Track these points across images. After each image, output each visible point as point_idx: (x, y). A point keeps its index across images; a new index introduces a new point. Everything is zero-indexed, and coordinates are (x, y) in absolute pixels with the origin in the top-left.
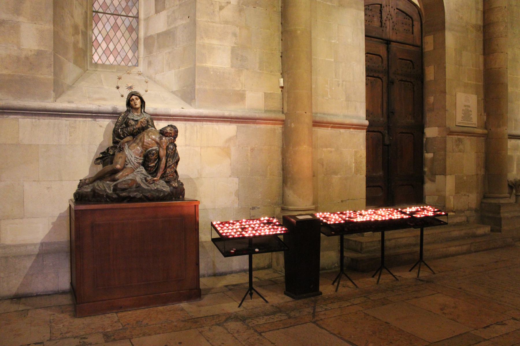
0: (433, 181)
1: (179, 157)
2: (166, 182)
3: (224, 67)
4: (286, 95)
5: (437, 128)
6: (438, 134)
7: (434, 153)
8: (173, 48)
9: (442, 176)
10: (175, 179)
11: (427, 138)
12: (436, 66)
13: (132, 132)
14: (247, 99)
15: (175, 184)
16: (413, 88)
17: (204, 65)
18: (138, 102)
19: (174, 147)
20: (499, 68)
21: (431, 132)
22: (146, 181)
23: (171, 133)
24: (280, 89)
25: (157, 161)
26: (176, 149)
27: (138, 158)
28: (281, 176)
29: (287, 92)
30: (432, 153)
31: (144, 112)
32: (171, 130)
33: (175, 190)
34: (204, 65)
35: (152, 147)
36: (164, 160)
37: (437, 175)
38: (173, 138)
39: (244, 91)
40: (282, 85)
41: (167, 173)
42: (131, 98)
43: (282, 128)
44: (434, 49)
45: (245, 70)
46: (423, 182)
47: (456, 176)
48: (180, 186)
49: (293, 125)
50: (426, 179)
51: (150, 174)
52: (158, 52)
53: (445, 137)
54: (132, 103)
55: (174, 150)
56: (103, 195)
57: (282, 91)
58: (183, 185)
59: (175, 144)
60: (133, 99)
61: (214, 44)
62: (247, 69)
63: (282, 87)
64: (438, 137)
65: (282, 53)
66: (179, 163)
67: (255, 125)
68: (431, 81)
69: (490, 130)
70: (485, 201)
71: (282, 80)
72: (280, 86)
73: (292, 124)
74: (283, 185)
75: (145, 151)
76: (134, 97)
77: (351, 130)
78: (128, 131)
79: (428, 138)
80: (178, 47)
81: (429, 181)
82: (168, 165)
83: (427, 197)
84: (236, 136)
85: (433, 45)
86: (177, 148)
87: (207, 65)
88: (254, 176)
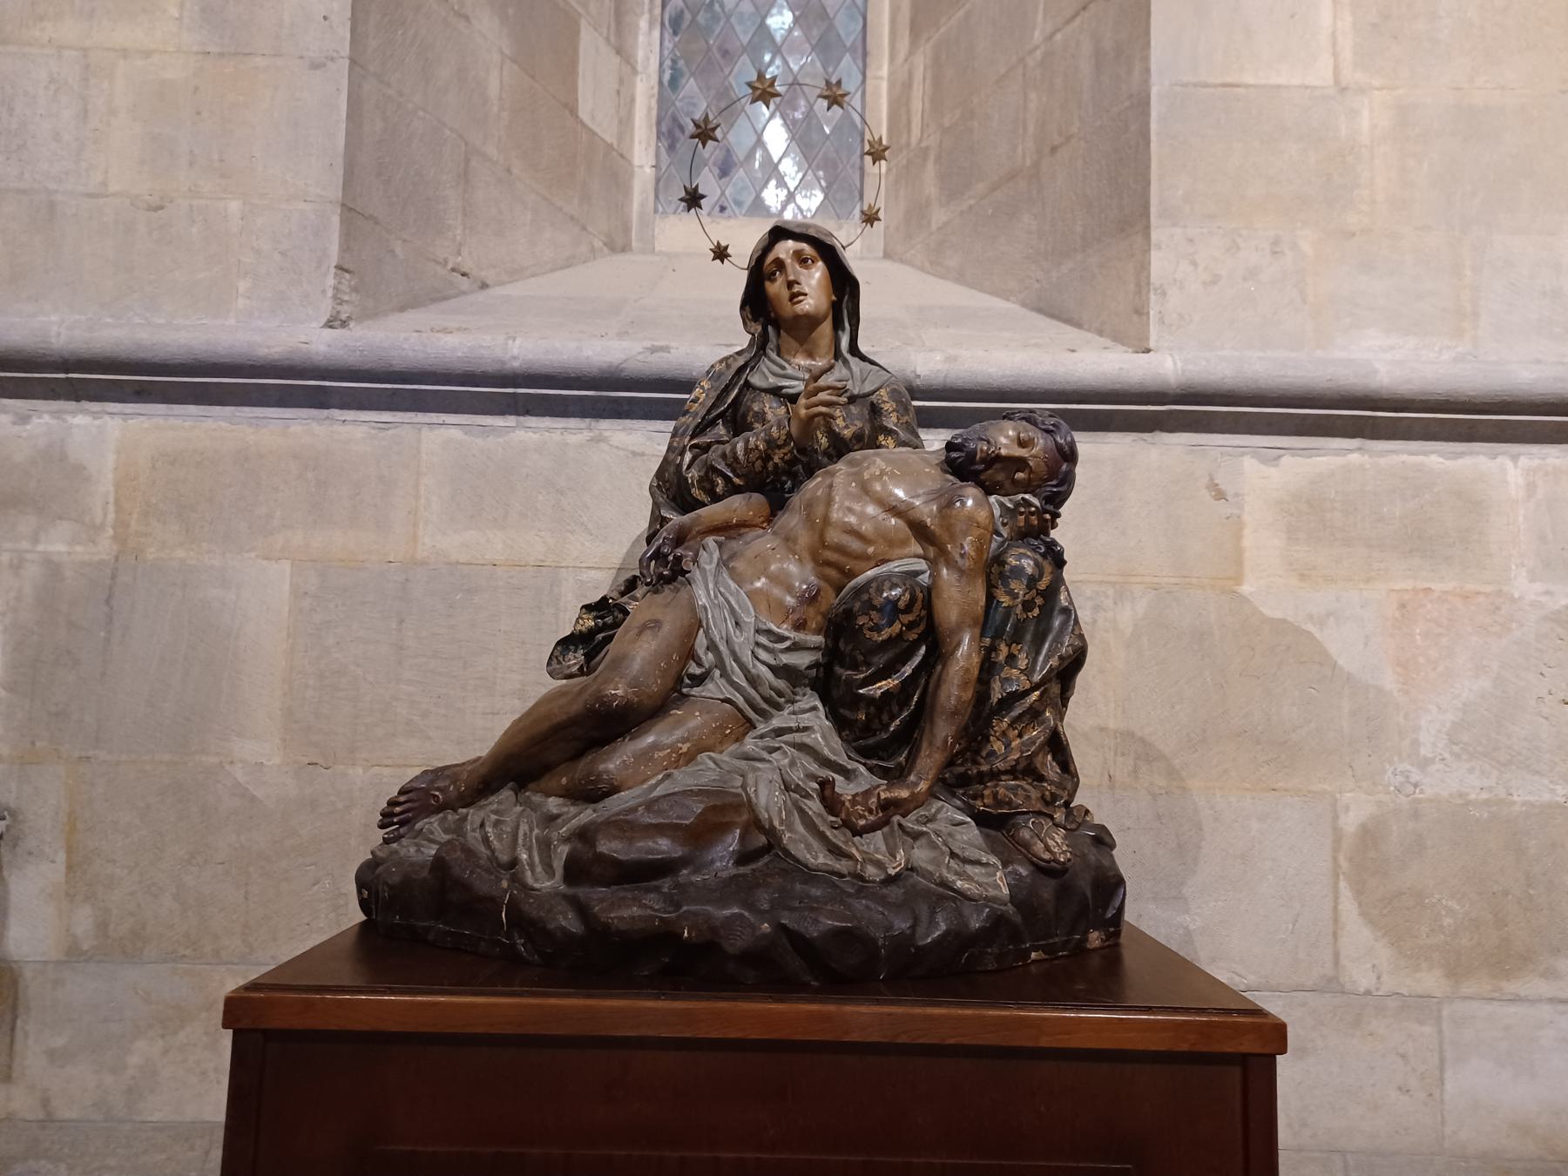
1: (1081, 637)
2: (982, 820)
10: (1050, 801)
13: (759, 464)
15: (1055, 844)
18: (814, 280)
19: (1048, 568)
22: (831, 802)
23: (1020, 463)
25: (917, 660)
26: (1058, 582)
27: (782, 639)
31: (854, 349)
32: (1022, 444)
33: (1047, 889)
35: (884, 561)
36: (965, 652)
38: (1036, 501)
41: (992, 753)
42: (770, 258)
48: (1093, 855)
51: (865, 753)
54: (776, 288)
55: (1042, 585)
56: (493, 902)
58: (1112, 846)
59: (1054, 543)
60: (780, 264)
66: (1081, 679)
75: (839, 589)
76: (785, 249)
78: (736, 458)
82: (997, 694)
86: (1067, 573)
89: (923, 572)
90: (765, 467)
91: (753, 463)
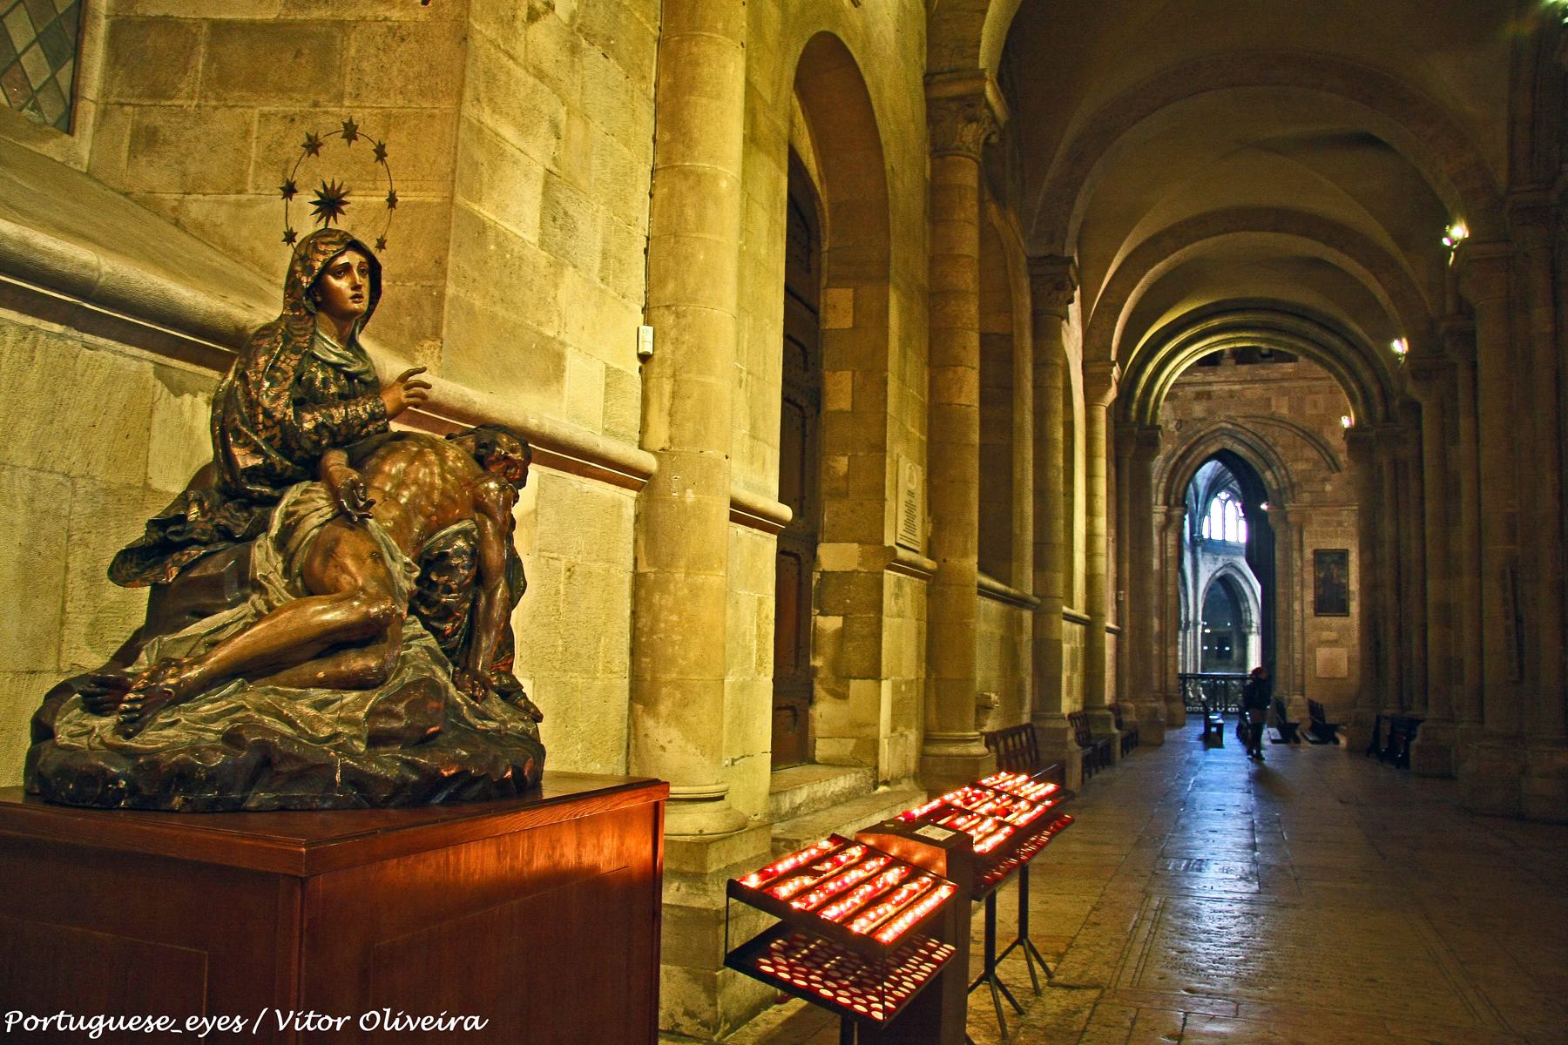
0: (840, 695)
3: (524, 236)
4: (667, 387)
5: (856, 545)
6: (860, 564)
7: (845, 616)
8: (316, 104)
9: (869, 683)
11: (823, 573)
12: (857, 374)
14: (567, 374)
16: (804, 425)
17: (476, 207)
20: (969, 406)
21: (834, 557)
24: (639, 364)
28: (627, 675)
29: (674, 375)
30: (839, 615)
34: (476, 207)
37: (855, 678)
39: (563, 344)
40: (647, 347)
43: (636, 500)
44: (855, 327)
45: (571, 269)
46: (811, 700)
47: (893, 682)
49: (690, 496)
50: (819, 691)
52: (214, 103)
53: (878, 573)
57: (640, 369)
61: (504, 139)
62: (575, 267)
63: (644, 358)
64: (859, 572)
65: (648, 239)
67: (581, 478)
68: (841, 412)
69: (945, 561)
70: (934, 750)
71: (647, 333)
72: (640, 351)
73: (689, 491)
74: (631, 709)
77: (756, 531)
79: (828, 573)
80: (347, 103)
81: (829, 697)
83: (819, 744)
84: (536, 511)
85: (851, 315)
87: (482, 211)
88: (570, 674)
89: (474, 530)
90: (360, 432)
91: (354, 428)
